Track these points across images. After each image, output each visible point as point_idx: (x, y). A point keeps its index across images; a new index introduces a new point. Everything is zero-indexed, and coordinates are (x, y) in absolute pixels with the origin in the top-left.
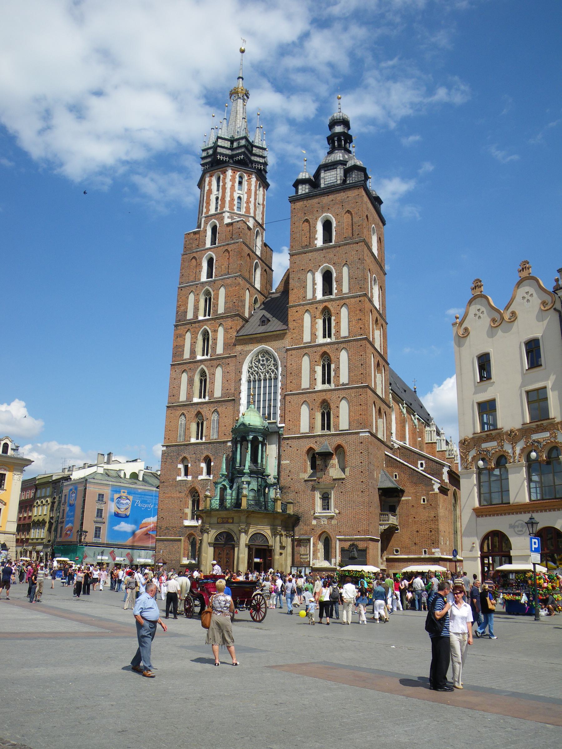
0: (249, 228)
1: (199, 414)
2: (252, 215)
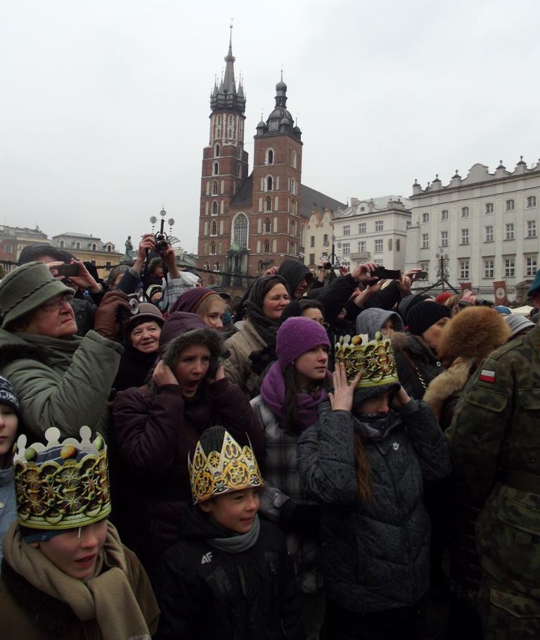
0: (234, 147)
1: (213, 242)
2: (237, 139)
